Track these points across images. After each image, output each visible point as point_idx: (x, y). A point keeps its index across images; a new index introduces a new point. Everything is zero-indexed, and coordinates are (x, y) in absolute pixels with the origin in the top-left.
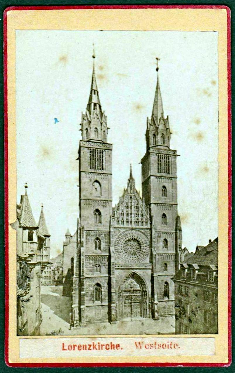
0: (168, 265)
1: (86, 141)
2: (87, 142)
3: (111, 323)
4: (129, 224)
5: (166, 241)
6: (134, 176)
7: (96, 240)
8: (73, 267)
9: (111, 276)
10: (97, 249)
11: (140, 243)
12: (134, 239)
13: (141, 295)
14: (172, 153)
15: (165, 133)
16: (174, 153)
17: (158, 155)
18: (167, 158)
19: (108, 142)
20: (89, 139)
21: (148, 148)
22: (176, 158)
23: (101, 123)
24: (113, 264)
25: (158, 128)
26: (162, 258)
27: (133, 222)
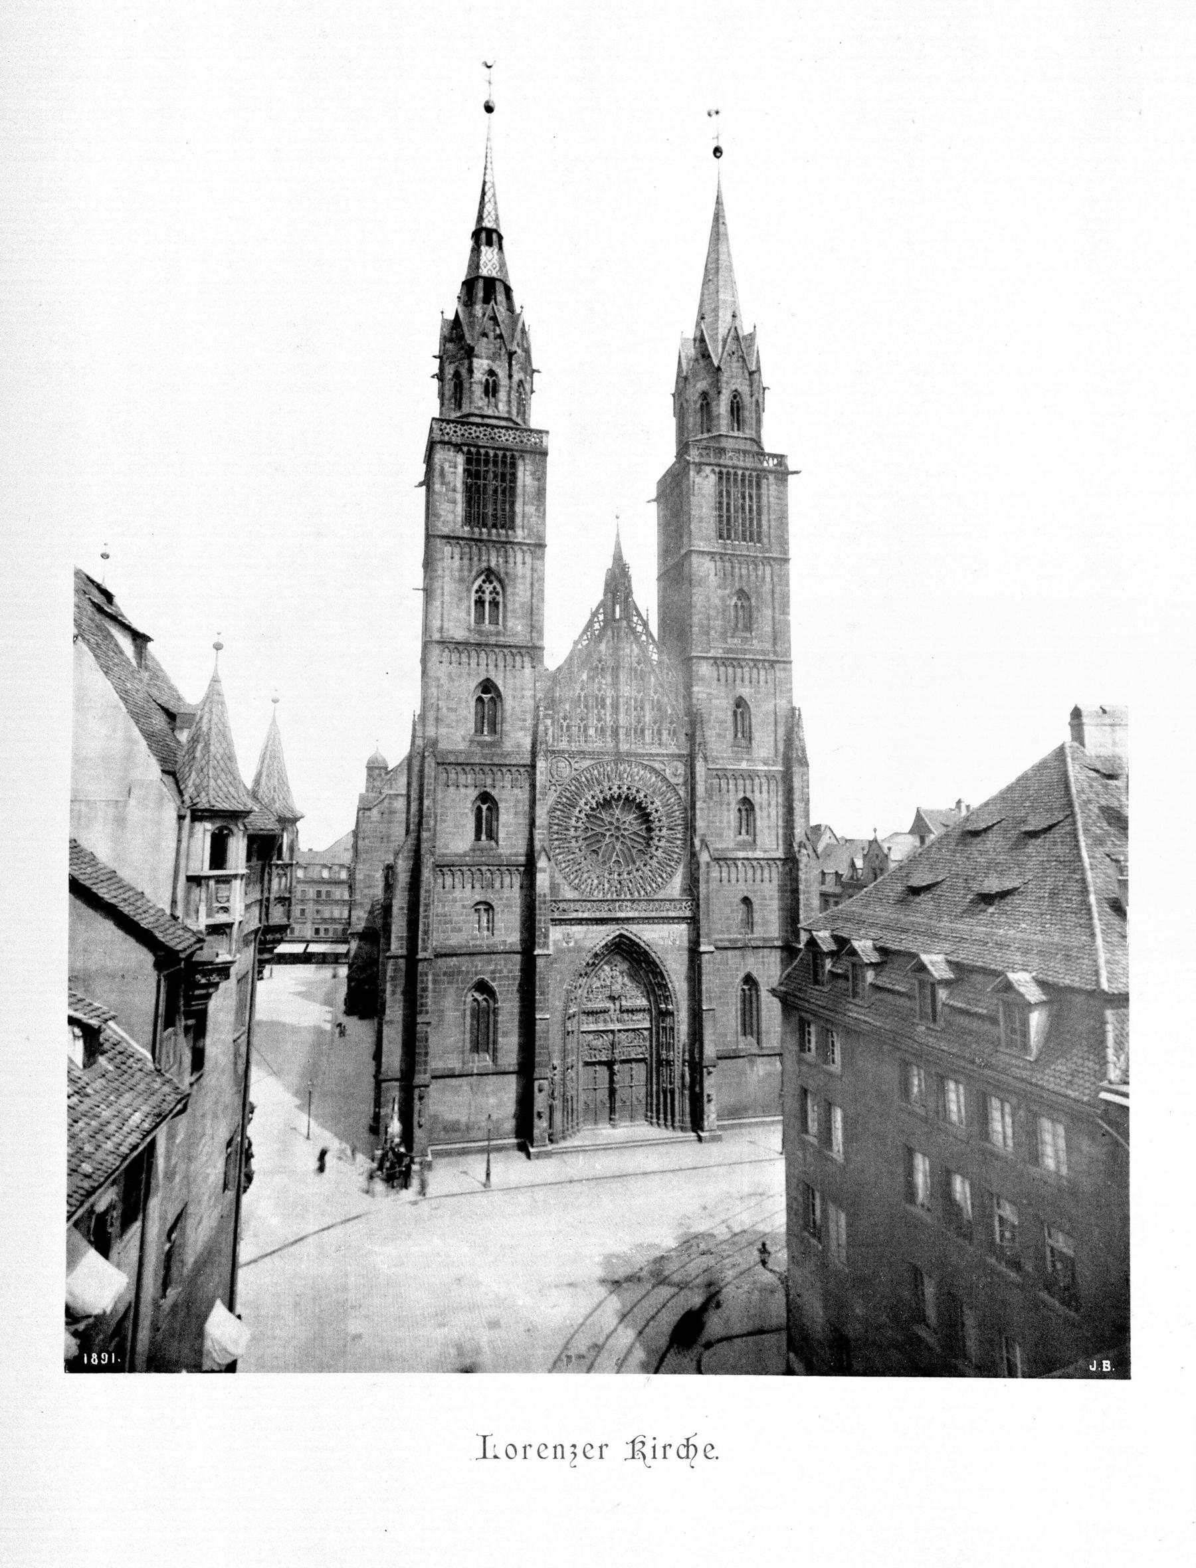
0: (755, 907)
1: (453, 422)
2: (458, 423)
3: (528, 1156)
4: (609, 739)
5: (747, 805)
6: (626, 558)
7: (479, 803)
8: (387, 909)
9: (536, 953)
10: (484, 837)
11: (649, 814)
12: (627, 798)
13: (650, 1029)
14: (771, 463)
15: (744, 389)
16: (780, 464)
17: (721, 473)
18: (750, 481)
19: (534, 424)
20: (466, 409)
21: (683, 447)
22: (786, 480)
23: (511, 355)
24: (545, 903)
25: (719, 369)
26: (733, 876)
27: (622, 731)
